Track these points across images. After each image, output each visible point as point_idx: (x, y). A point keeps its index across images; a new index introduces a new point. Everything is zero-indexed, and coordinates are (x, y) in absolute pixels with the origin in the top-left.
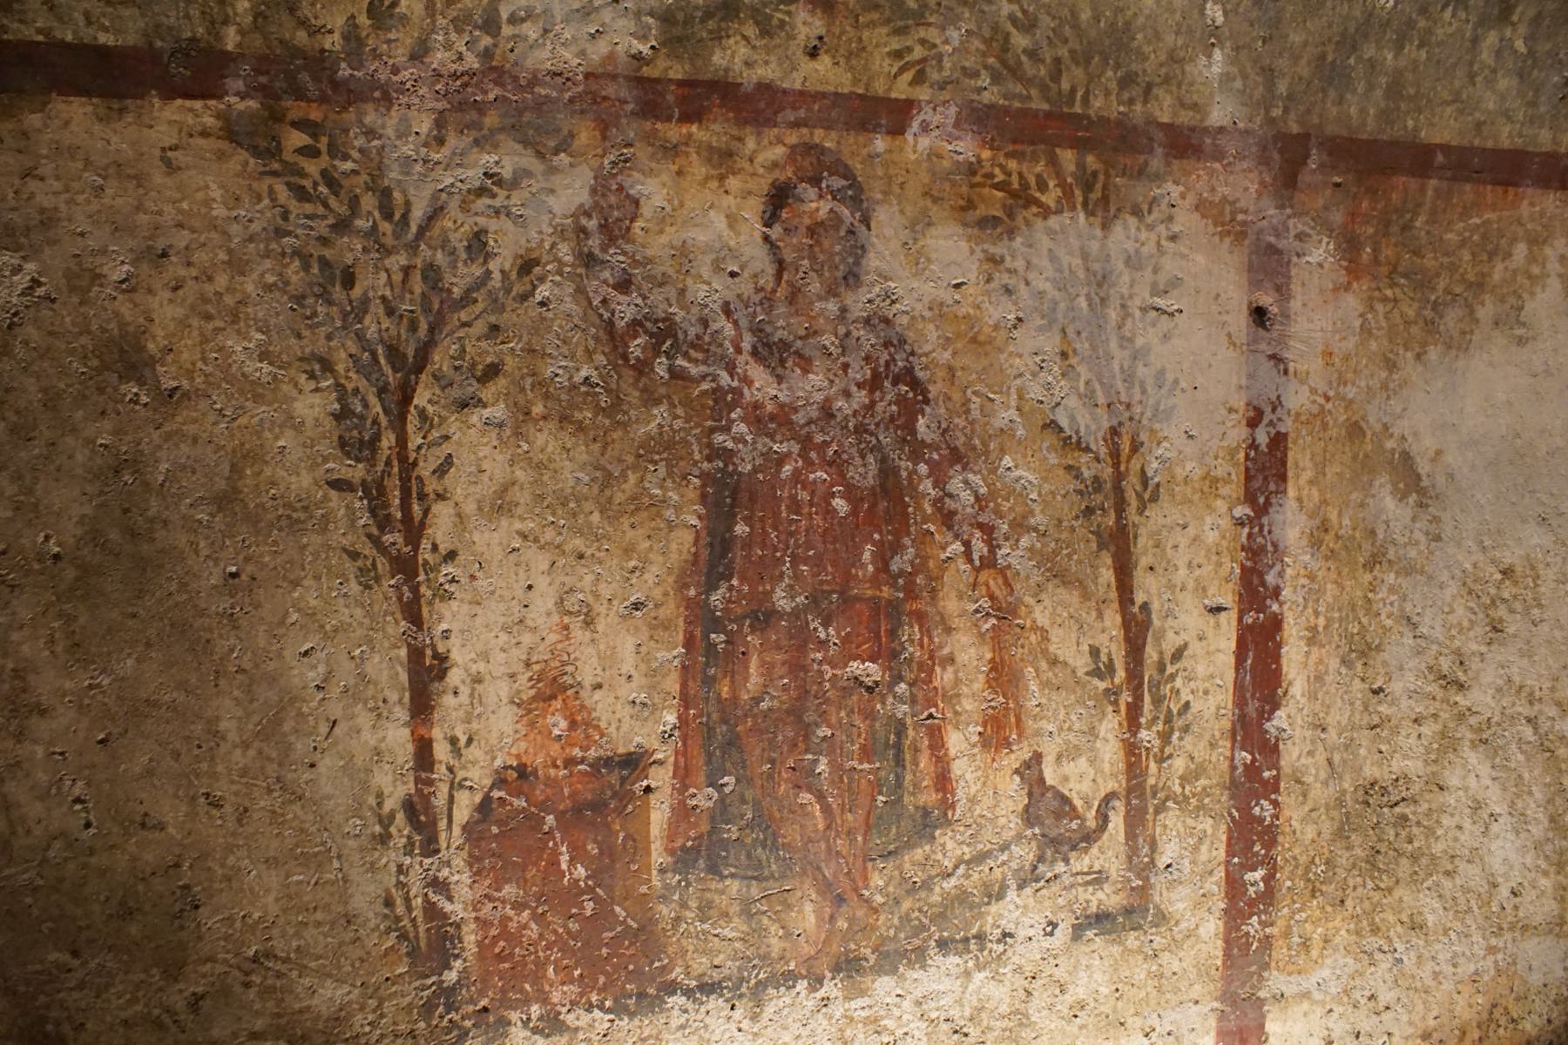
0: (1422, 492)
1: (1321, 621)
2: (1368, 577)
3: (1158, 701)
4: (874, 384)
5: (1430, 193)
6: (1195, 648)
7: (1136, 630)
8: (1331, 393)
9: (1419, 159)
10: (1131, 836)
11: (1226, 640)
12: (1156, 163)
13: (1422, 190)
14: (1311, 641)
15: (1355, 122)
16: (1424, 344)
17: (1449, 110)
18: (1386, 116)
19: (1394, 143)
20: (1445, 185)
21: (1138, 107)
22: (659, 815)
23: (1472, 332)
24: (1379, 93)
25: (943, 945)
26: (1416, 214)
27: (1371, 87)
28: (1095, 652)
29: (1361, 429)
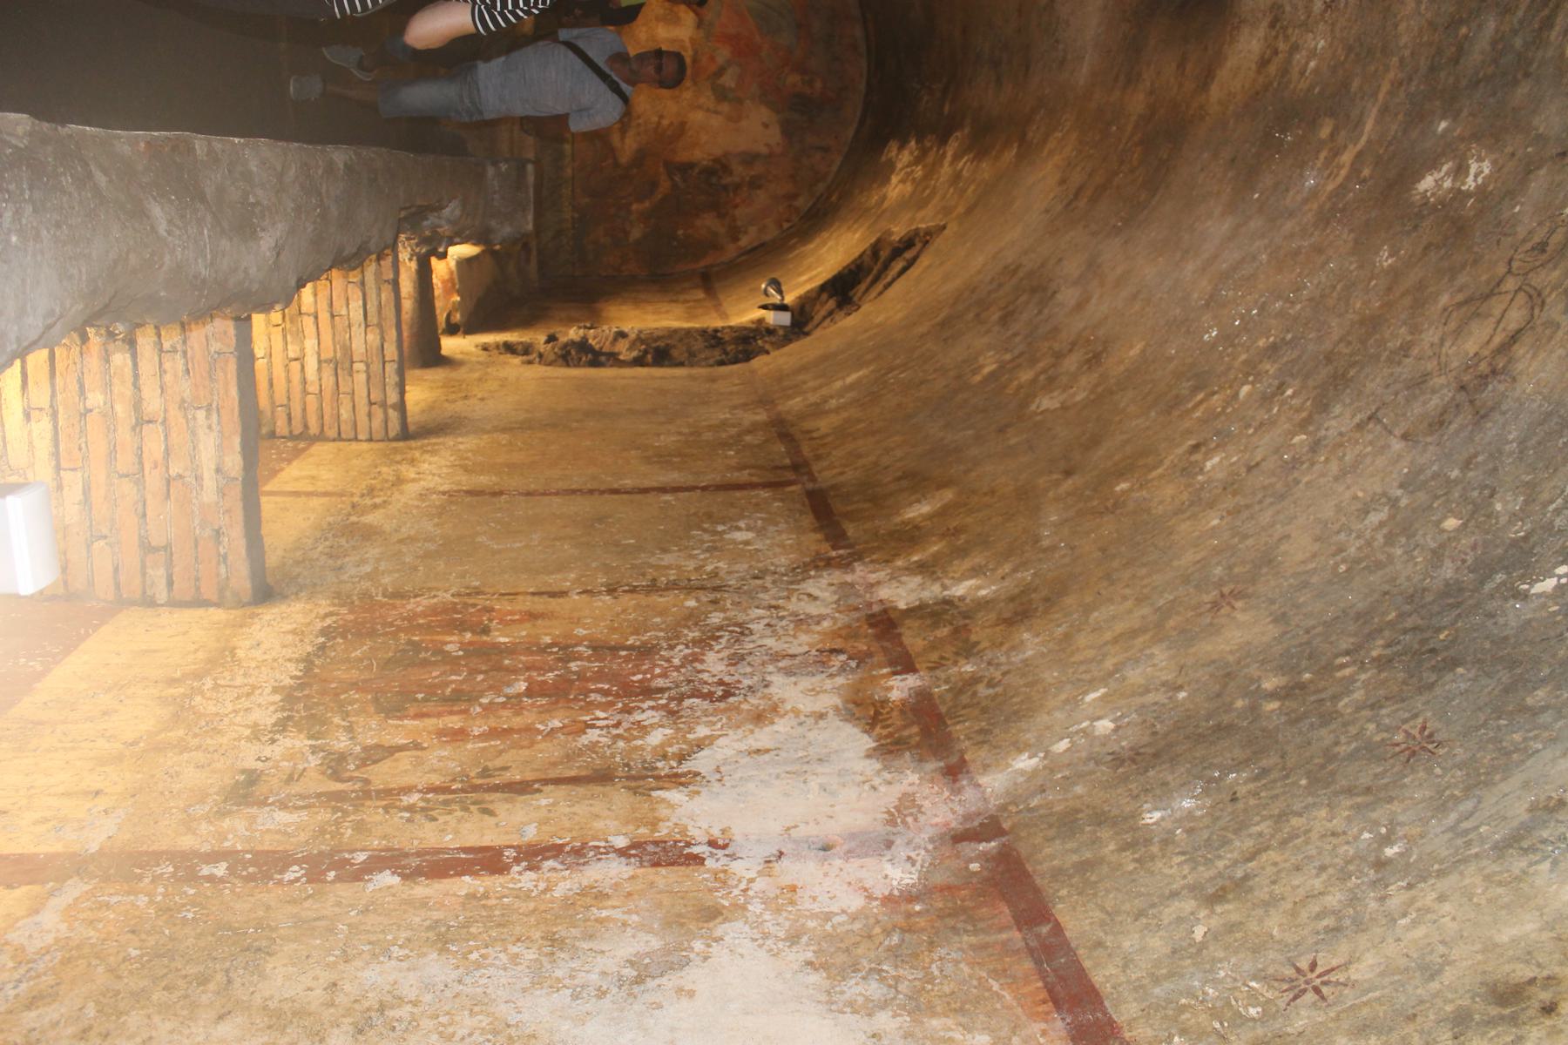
0: (639, 980)
1: (492, 902)
2: (537, 935)
3: (446, 803)
4: (721, 683)
5: (1004, 936)
6: (491, 821)
7: (522, 788)
8: (751, 893)
9: (1033, 912)
10: (319, 795)
11: (490, 839)
12: (932, 765)
13: (1001, 929)
14: (472, 896)
15: (1039, 856)
16: (824, 967)
17: (1098, 914)
18: (1057, 874)
19: (1037, 891)
20: (1021, 944)
21: (967, 743)
22: (448, 639)
23: (855, 1012)
24: (1075, 858)
25: (289, 718)
26: (976, 932)
27: (1074, 851)
28: (505, 769)
29: (715, 917)
